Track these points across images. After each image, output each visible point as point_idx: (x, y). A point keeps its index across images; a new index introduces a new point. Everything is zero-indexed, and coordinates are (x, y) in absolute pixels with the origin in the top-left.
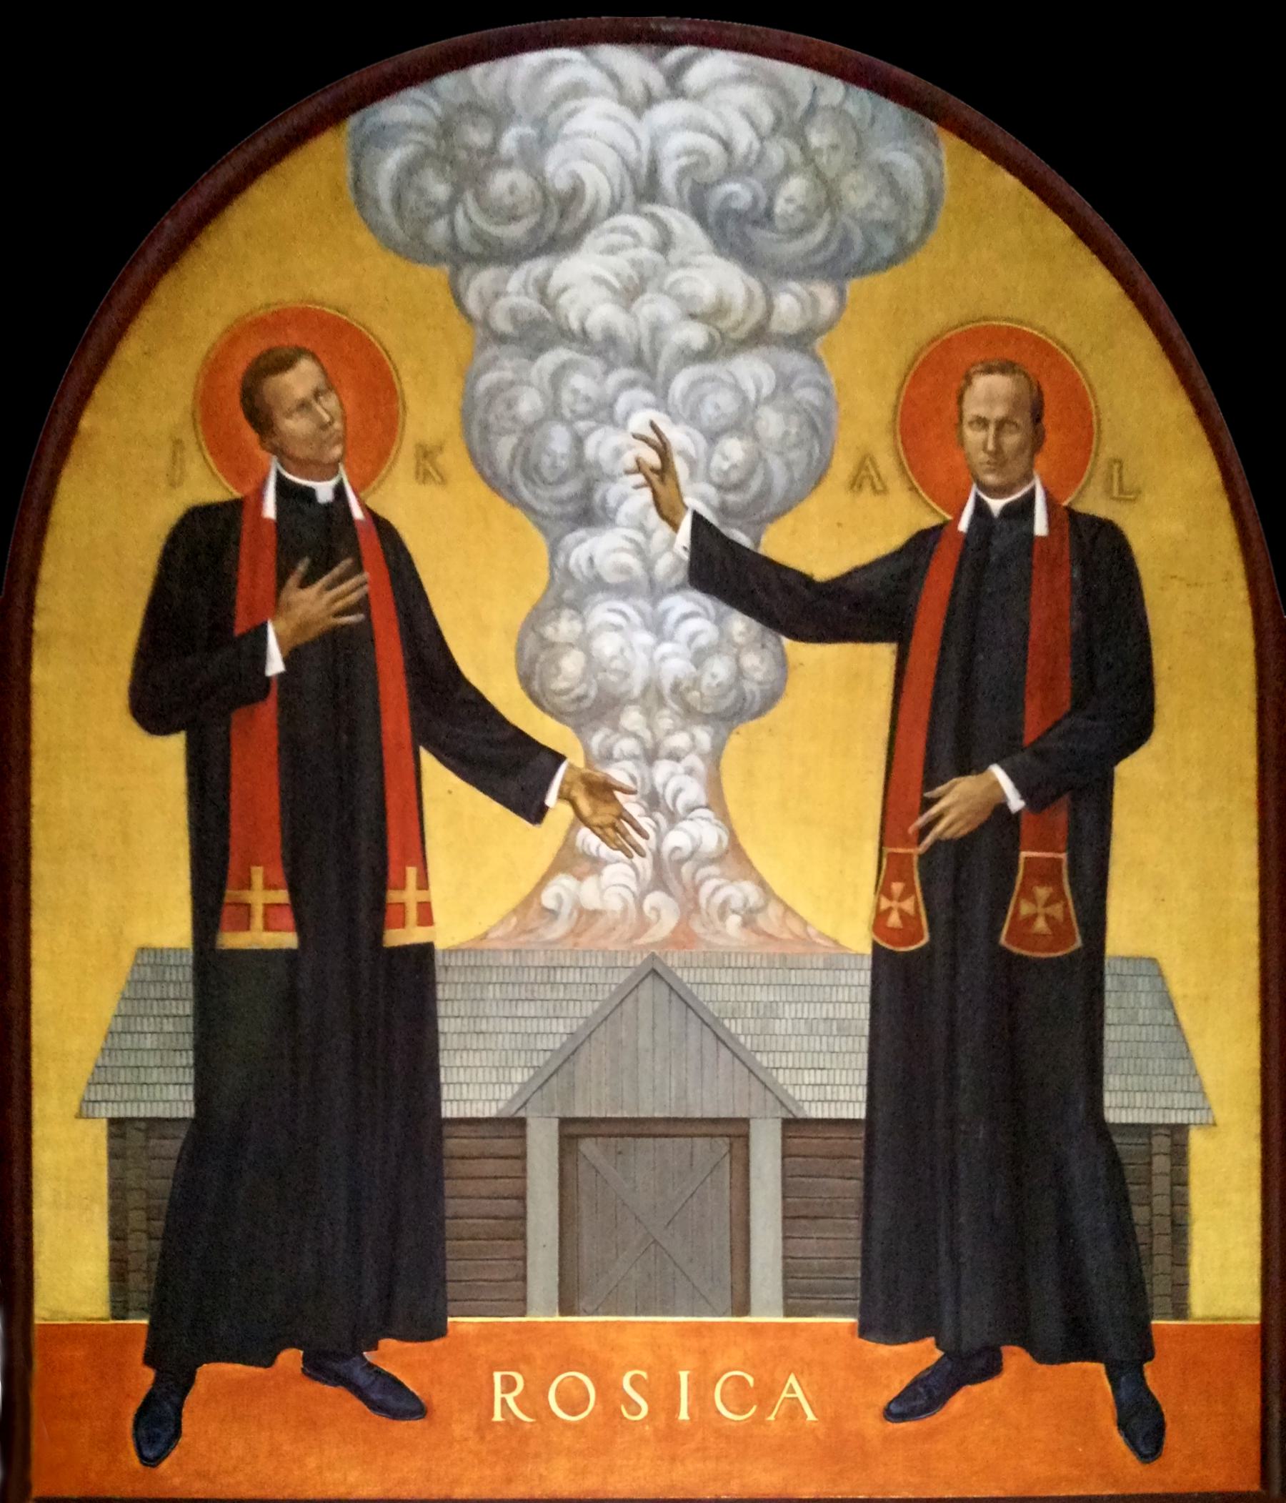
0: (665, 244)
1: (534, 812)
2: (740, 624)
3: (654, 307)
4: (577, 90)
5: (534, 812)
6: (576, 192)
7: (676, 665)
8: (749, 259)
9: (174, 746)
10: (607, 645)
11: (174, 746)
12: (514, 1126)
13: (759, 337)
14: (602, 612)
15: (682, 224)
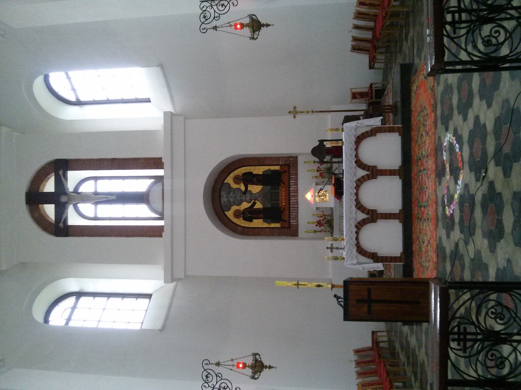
0: (230, 196)
1: (256, 202)
2: (247, 192)
3: (233, 197)
4: (223, 200)
5: (256, 202)
6: (228, 200)
7: (249, 196)
8: (231, 192)
9: (254, 220)
10: (248, 199)
11: (254, 220)
12: (271, 204)
13: (234, 191)
14: (247, 199)
15: (229, 195)
